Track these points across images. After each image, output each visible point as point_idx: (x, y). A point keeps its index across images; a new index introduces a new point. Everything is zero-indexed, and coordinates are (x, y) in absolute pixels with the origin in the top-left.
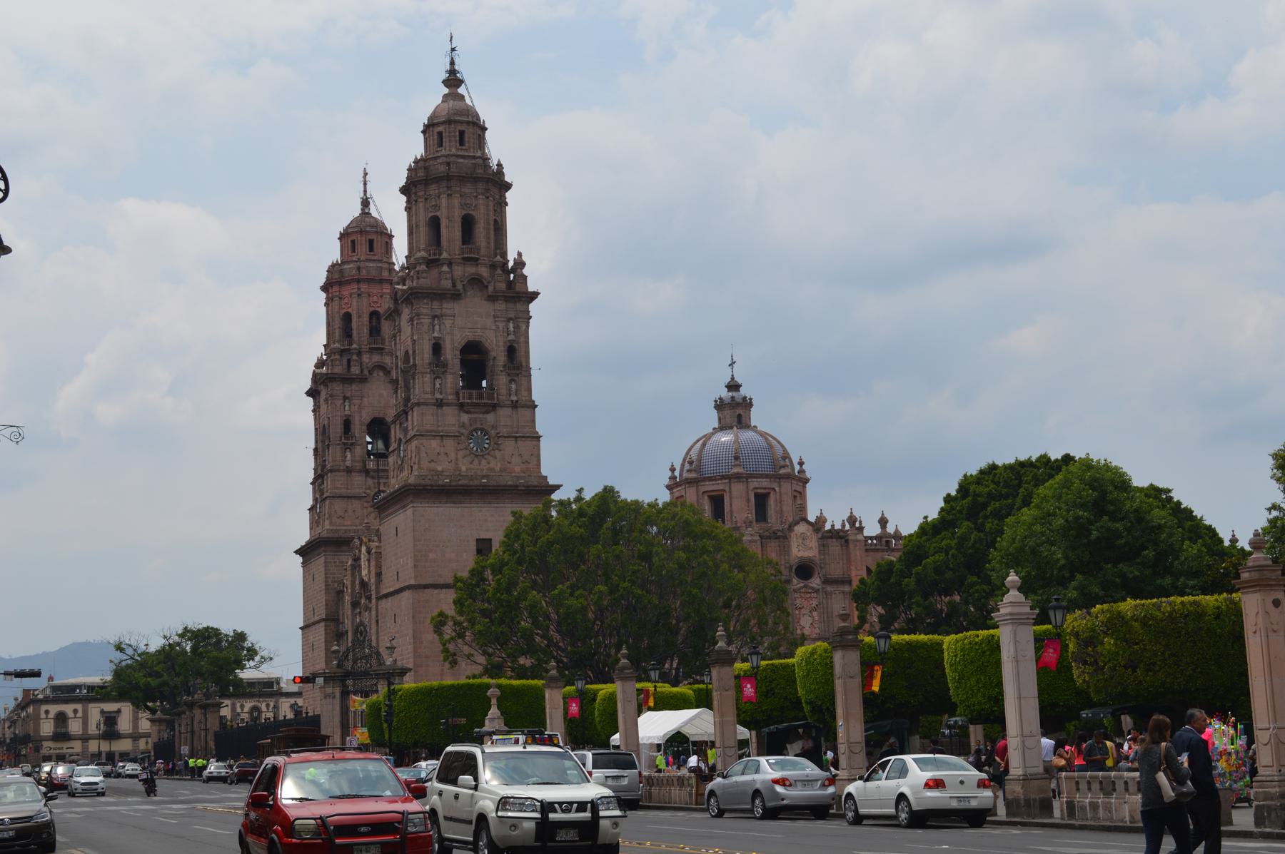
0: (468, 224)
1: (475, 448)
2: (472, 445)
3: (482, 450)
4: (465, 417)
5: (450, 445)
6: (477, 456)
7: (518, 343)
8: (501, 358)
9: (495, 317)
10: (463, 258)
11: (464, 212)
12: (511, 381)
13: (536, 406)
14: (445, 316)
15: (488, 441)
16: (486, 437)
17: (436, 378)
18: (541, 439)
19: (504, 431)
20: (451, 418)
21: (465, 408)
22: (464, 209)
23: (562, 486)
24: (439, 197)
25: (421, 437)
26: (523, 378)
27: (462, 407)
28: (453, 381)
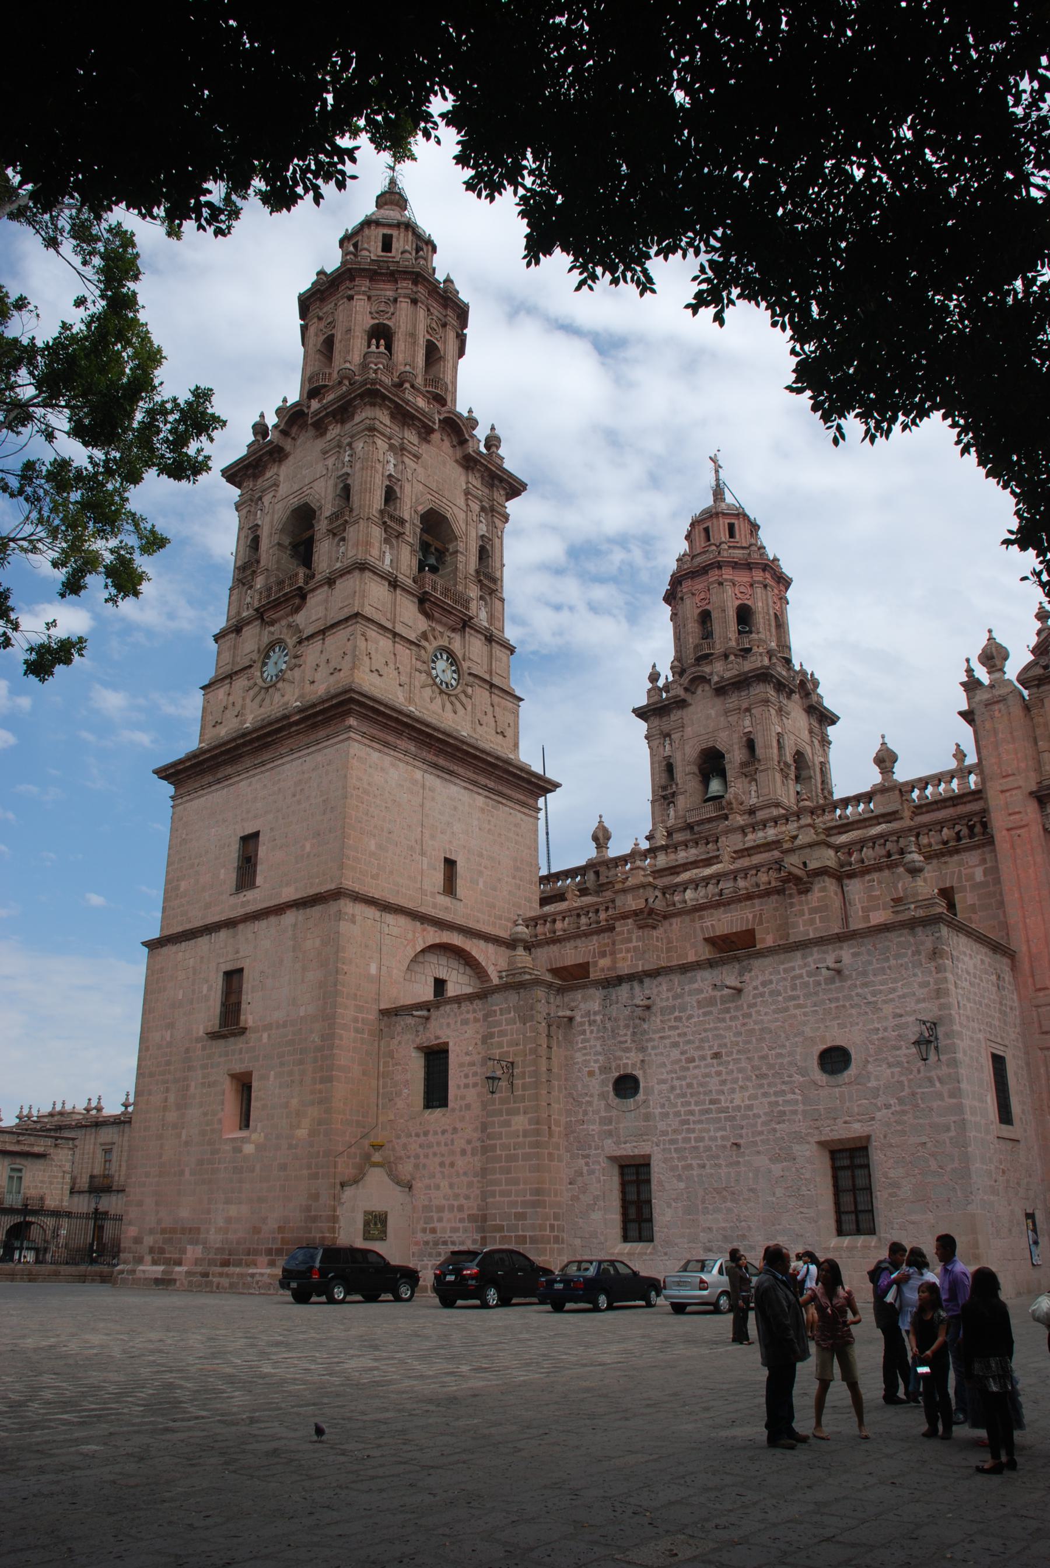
0: (432, 354)
3: (447, 684)
4: (422, 624)
5: (404, 653)
6: (441, 692)
10: (427, 392)
12: (482, 598)
13: (512, 650)
15: (455, 676)
16: (453, 668)
18: (521, 703)
21: (427, 605)
23: (557, 785)
24: (395, 300)
25: (363, 622)
26: (497, 602)
27: (424, 602)
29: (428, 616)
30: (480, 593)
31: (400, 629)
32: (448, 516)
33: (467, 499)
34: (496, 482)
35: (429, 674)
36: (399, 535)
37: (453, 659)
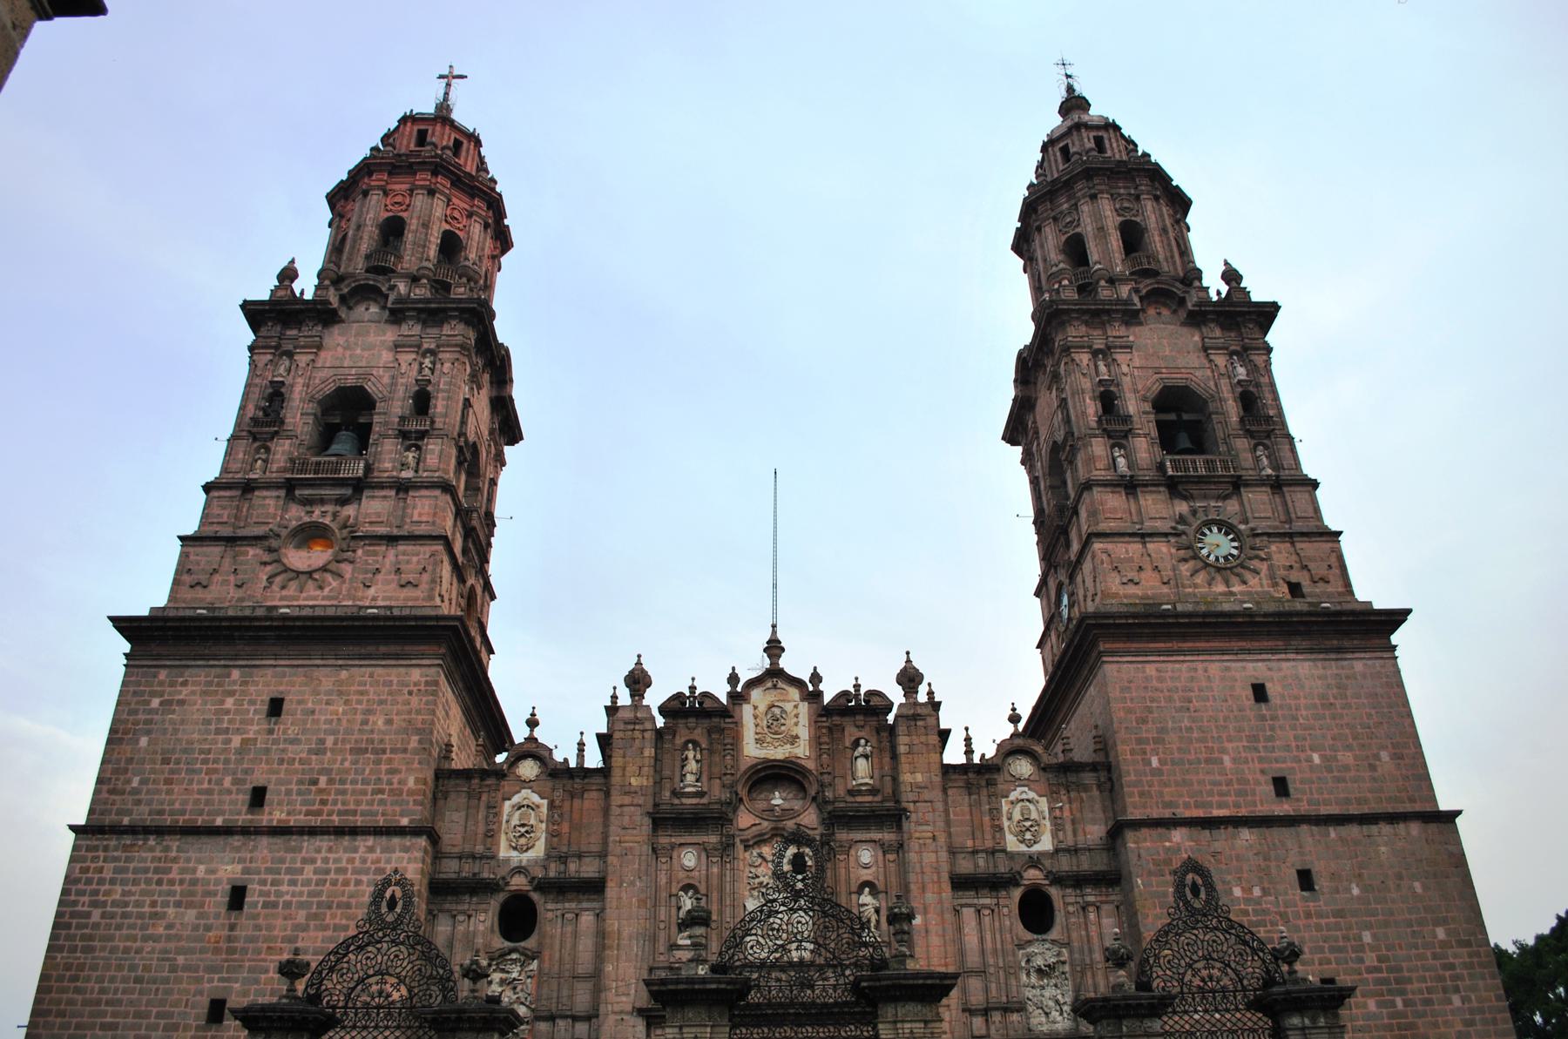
1: (1212, 558)
2: (1204, 552)
4: (1182, 507)
5: (1160, 548)
6: (1219, 569)
7: (1258, 385)
8: (1233, 410)
9: (1205, 349)
11: (1121, 219)
13: (1314, 484)
14: (1116, 347)
15: (1236, 544)
16: (1231, 536)
17: (1112, 447)
19: (1262, 526)
20: (1157, 508)
21: (1180, 487)
22: (1119, 215)
23: (1409, 611)
27: (1175, 487)
28: (1144, 449)
29: (1185, 498)
30: (1253, 442)
31: (1149, 526)
32: (1188, 383)
33: (1208, 355)
34: (1239, 319)
35: (1196, 557)
36: (1126, 434)
37: (1227, 528)
